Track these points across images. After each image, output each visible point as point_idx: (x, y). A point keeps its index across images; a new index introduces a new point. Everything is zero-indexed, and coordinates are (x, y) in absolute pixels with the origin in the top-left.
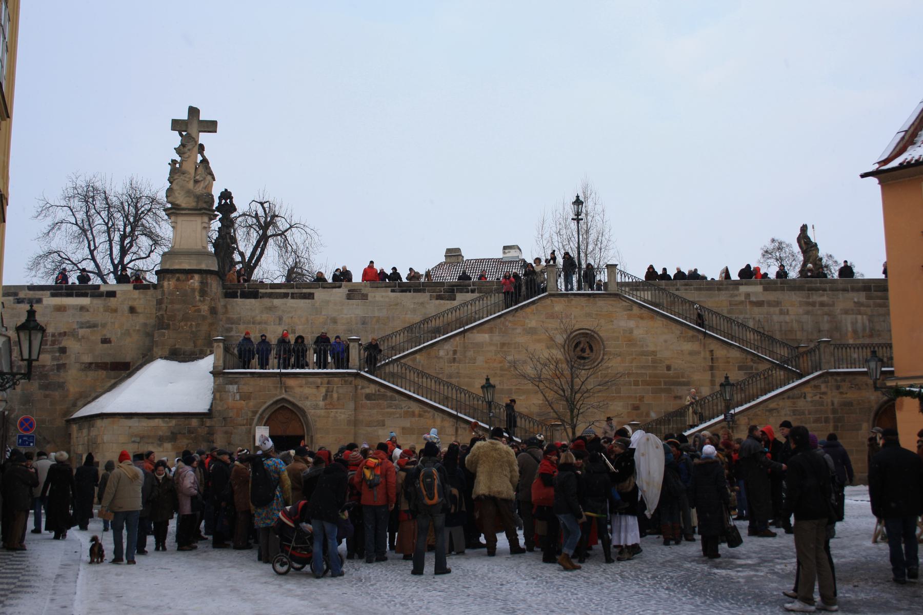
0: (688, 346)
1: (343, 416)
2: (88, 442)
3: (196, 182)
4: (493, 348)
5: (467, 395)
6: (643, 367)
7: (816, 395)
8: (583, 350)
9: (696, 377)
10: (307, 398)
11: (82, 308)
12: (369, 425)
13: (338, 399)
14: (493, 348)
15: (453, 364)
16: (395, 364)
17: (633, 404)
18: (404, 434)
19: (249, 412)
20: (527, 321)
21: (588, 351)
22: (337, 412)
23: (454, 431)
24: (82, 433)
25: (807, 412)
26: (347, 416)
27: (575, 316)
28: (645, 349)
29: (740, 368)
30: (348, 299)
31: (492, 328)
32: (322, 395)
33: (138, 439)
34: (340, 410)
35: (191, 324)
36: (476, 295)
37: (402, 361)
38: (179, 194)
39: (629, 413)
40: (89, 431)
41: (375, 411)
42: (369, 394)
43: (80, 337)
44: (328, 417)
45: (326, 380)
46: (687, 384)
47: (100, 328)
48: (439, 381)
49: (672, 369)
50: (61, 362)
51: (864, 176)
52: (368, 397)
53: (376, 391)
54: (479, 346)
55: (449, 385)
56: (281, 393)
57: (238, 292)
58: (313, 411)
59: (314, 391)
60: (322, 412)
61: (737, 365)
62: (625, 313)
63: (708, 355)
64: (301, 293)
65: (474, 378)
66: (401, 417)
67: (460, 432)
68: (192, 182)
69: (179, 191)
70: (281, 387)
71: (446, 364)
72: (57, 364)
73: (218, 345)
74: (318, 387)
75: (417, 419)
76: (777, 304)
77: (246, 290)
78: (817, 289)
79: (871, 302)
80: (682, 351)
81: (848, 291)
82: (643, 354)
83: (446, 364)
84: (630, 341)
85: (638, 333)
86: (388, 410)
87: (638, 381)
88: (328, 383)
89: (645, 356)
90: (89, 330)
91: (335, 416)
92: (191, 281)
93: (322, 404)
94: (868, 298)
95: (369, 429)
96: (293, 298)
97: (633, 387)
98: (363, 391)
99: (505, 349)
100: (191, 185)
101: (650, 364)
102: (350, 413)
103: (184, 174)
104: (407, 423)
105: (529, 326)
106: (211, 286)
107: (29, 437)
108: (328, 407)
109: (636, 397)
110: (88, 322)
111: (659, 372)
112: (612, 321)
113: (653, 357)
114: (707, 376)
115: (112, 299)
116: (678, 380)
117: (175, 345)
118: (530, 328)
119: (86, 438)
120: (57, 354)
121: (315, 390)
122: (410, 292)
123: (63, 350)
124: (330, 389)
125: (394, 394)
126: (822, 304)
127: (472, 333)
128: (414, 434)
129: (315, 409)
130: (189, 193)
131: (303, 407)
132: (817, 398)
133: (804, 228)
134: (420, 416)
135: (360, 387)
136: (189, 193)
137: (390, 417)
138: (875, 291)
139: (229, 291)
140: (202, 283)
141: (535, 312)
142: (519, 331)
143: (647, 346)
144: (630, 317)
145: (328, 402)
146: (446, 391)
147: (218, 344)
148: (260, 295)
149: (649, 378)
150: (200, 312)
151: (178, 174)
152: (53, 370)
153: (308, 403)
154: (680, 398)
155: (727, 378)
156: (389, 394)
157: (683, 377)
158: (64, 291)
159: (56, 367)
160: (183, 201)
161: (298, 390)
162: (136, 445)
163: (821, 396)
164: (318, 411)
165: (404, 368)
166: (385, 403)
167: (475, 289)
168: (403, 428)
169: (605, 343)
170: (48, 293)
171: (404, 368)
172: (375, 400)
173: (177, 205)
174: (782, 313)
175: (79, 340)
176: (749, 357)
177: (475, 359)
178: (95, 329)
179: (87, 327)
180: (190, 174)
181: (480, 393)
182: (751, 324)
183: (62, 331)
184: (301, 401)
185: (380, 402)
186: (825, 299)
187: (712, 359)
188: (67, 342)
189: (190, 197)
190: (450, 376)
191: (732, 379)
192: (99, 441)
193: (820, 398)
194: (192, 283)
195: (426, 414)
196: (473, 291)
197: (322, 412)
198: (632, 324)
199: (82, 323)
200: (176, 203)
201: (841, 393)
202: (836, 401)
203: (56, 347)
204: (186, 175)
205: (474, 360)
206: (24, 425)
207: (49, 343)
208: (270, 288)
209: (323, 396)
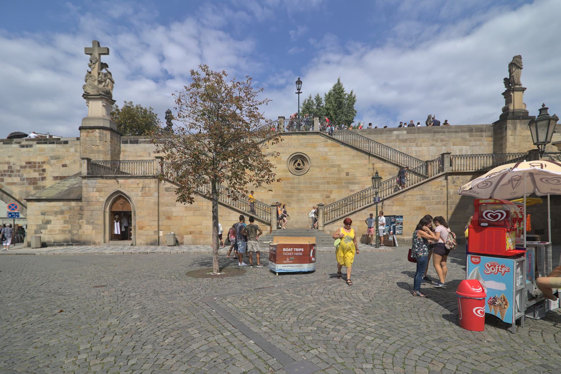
1: (152, 200)
7: (438, 188)
8: (299, 165)
11: (53, 150)
12: (167, 205)
17: (326, 195)
18: (186, 210)
21: (302, 165)
22: (148, 198)
25: (431, 198)
28: (334, 163)
38: (89, 87)
39: (323, 199)
41: (170, 198)
44: (143, 201)
46: (359, 183)
47: (61, 159)
49: (350, 175)
50: (43, 176)
60: (140, 198)
69: (88, 86)
72: (42, 177)
73: (84, 162)
74: (138, 184)
77: (133, 139)
78: (438, 132)
81: (459, 132)
82: (333, 166)
84: (325, 159)
97: (326, 185)
98: (164, 186)
100: (96, 83)
102: (156, 199)
107: (15, 213)
108: (143, 195)
110: (55, 156)
113: (338, 168)
120: (41, 172)
123: (44, 170)
128: (191, 210)
130: (94, 87)
131: (130, 196)
138: (475, 132)
139: (124, 140)
144: (326, 146)
148: (139, 142)
149: (336, 180)
160: (91, 91)
163: (442, 188)
164: (138, 198)
170: (35, 142)
173: (88, 93)
175: (51, 165)
178: (59, 160)
180: (95, 77)
183: (43, 161)
188: (45, 166)
197: (140, 198)
198: (326, 149)
201: (456, 186)
203: (41, 169)
204: (92, 77)
206: (15, 207)
207: (37, 167)
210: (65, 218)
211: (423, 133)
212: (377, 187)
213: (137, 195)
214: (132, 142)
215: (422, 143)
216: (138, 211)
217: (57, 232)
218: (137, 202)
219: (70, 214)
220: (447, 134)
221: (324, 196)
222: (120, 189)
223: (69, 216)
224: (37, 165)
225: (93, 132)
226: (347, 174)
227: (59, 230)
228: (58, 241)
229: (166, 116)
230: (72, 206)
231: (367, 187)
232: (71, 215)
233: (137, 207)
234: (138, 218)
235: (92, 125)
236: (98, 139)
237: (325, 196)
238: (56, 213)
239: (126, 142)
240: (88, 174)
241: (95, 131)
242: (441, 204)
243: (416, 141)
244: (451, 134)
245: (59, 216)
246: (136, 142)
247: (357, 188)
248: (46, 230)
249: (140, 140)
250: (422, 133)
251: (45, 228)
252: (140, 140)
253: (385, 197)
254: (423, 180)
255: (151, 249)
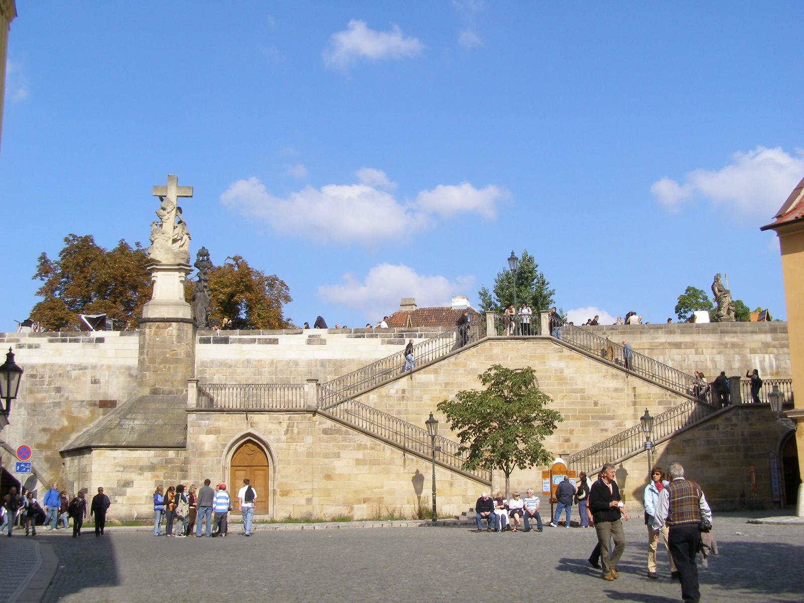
0: (612, 384)
1: (302, 449)
2: (78, 471)
3: (175, 241)
4: (438, 388)
5: (414, 430)
6: (573, 403)
7: (727, 427)
9: (620, 412)
10: (271, 432)
13: (298, 433)
14: (438, 388)
15: (401, 402)
16: (349, 403)
17: (564, 437)
19: (219, 445)
20: (468, 363)
23: (403, 461)
24: (74, 462)
25: (720, 442)
26: (306, 449)
27: (511, 358)
29: (660, 403)
30: (308, 344)
31: (437, 369)
32: (284, 430)
33: (121, 469)
34: (299, 444)
35: (169, 367)
36: (423, 340)
37: (356, 399)
39: (560, 444)
40: (79, 462)
42: (326, 428)
43: (73, 378)
44: (290, 449)
45: (287, 416)
46: (611, 418)
48: (389, 418)
49: (599, 405)
51: (764, 229)
52: (325, 432)
53: (332, 426)
54: (424, 386)
55: (398, 420)
56: (247, 429)
57: (211, 338)
58: (276, 444)
59: (277, 426)
60: (284, 445)
61: (657, 400)
62: (557, 354)
63: (631, 393)
64: (267, 339)
65: (421, 415)
66: (355, 450)
67: (407, 463)
68: (171, 241)
70: (248, 423)
71: (396, 402)
73: (192, 386)
74: (280, 422)
75: (369, 451)
76: (693, 345)
77: (219, 336)
78: (727, 332)
79: (776, 342)
80: (608, 388)
82: (574, 391)
83: (396, 402)
84: (561, 380)
85: (568, 373)
86: (343, 443)
87: (569, 416)
88: (289, 419)
89: (574, 393)
90: (81, 372)
91: (295, 449)
92: (169, 328)
93: (284, 437)
94: (774, 339)
95: (326, 460)
96: (259, 343)
99: (449, 388)
101: (579, 401)
103: (163, 234)
104: (359, 455)
105: (470, 367)
106: (187, 333)
108: (289, 440)
109: (567, 430)
110: (80, 365)
111: (586, 407)
112: (545, 362)
114: (630, 411)
115: (101, 344)
116: (605, 414)
117: (155, 385)
118: (471, 369)
119: (77, 467)
121: (278, 425)
122: (364, 337)
124: (291, 425)
125: (349, 430)
126: (734, 345)
127: (419, 374)
128: (366, 465)
129: (277, 442)
130: (168, 250)
132: (729, 429)
133: (717, 279)
134: (372, 448)
135: (317, 423)
136: (168, 250)
137: (344, 450)
140: (179, 330)
141: (475, 354)
142: (461, 371)
143: (576, 384)
144: (561, 358)
145: (288, 436)
146: (395, 425)
147: (192, 384)
149: (579, 413)
150: (177, 356)
151: (158, 234)
152: (49, 408)
153: (272, 437)
154: (606, 430)
155: (647, 412)
156: (344, 428)
157: (608, 412)
158: (60, 337)
159: (52, 404)
161: (261, 426)
162: (120, 474)
163: (733, 427)
165: (357, 406)
166: (340, 437)
167: (422, 335)
168: (357, 460)
169: (539, 381)
171: (357, 406)
172: (331, 434)
174: (697, 353)
176: (669, 393)
177: (422, 397)
179: (79, 370)
181: (425, 427)
182: (670, 364)
184: (266, 435)
185: (336, 436)
186: (735, 340)
187: (635, 395)
189: (168, 254)
190: (399, 413)
191: (651, 414)
192: (88, 470)
193: (732, 429)
194: (170, 330)
195: (378, 447)
196: (420, 336)
197: (284, 445)
198: (562, 364)
199: (75, 366)
200: (157, 259)
202: (746, 431)
204: (165, 234)
205: (420, 399)
208: (239, 335)
209: (285, 431)
210: (158, 476)
211: (706, 333)
212: (648, 430)
213: (278, 440)
214: (218, 341)
215: (704, 350)
216: (281, 466)
217: (143, 502)
218: (280, 451)
219: (166, 471)
220: (740, 335)
221: (562, 440)
222: (251, 430)
223: (165, 474)
224: (47, 379)
225: (166, 328)
226: (596, 404)
227: (147, 497)
228: (145, 516)
229: (198, 260)
230: (169, 457)
231: (629, 424)
232: (167, 473)
233: (279, 460)
234: (279, 477)
235: (166, 316)
236: (174, 339)
237: (563, 439)
238: (142, 469)
239: (206, 341)
240: (197, 406)
241: (170, 326)
242: (733, 451)
243: (696, 347)
244: (745, 335)
245: (148, 474)
246: (225, 341)
247: (611, 429)
248: (124, 497)
249: (231, 337)
250: (703, 333)
251: (123, 494)
252: (231, 337)
253: (656, 442)
254: (707, 415)
255: (179, 537)
